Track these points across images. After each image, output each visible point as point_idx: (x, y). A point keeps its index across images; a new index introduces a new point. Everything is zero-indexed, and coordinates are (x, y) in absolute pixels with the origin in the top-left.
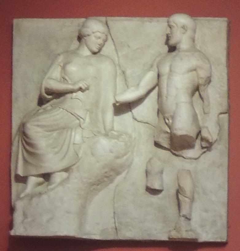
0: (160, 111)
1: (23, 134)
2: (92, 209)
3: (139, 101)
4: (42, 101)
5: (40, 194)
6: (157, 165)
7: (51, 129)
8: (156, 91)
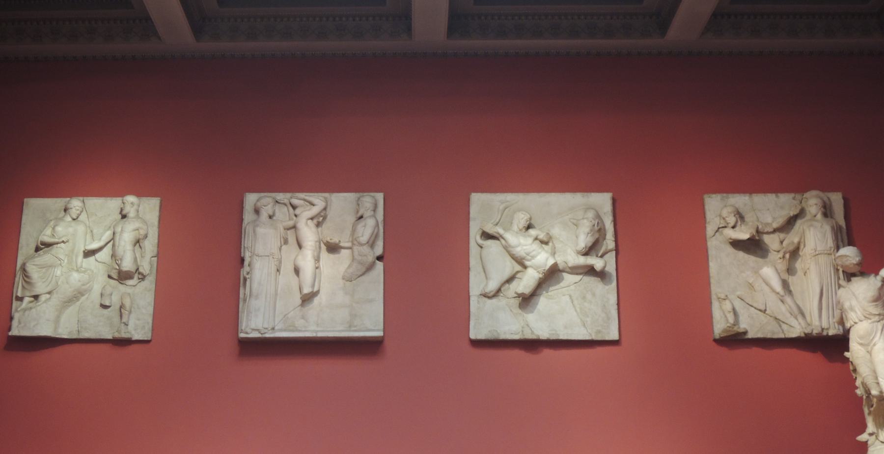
0: (113, 256)
1: (24, 269)
2: (64, 318)
3: (100, 249)
4: (37, 249)
5: (31, 308)
6: (109, 290)
7: (42, 267)
8: (111, 243)
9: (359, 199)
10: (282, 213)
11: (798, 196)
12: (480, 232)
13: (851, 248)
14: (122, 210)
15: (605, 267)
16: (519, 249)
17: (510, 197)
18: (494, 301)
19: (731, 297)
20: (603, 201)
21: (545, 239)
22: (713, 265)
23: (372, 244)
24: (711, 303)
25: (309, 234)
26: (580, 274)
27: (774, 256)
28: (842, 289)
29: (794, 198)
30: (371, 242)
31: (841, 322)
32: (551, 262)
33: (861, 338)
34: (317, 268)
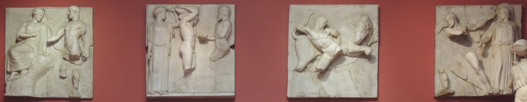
0: (66, 45)
1: (10, 54)
2: (38, 85)
3: (57, 41)
4: (17, 41)
5: (17, 79)
6: (64, 67)
7: (21, 53)
8: (64, 37)
9: (219, 8)
10: (171, 18)
11: (494, 7)
12: (295, 30)
13: (523, 40)
14: (69, 16)
15: (371, 52)
16: (319, 41)
17: (314, 7)
18: (303, 74)
19: (447, 71)
20: (372, 10)
21: (335, 35)
22: (438, 51)
23: (228, 38)
24: (434, 75)
25: (188, 31)
26: (356, 57)
27: (475, 46)
28: (514, 66)
29: (491, 8)
30: (227, 36)
31: (512, 86)
32: (338, 49)
33: (522, 96)
34: (193, 53)
